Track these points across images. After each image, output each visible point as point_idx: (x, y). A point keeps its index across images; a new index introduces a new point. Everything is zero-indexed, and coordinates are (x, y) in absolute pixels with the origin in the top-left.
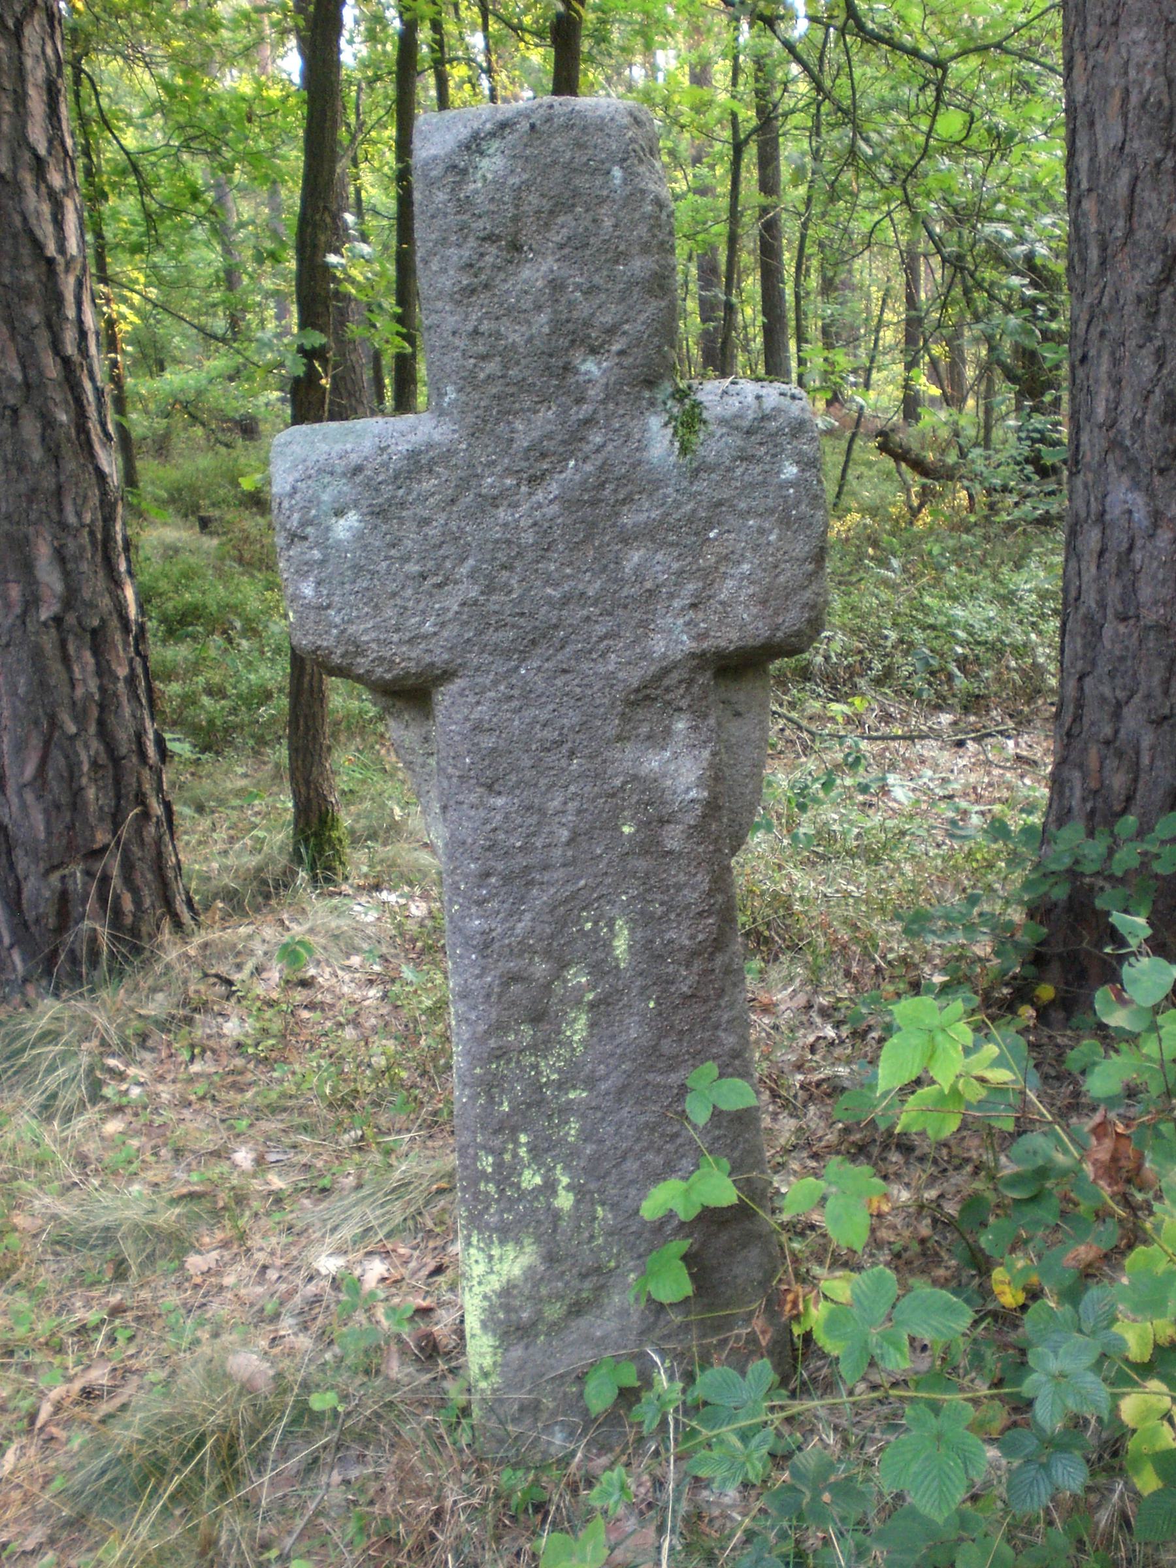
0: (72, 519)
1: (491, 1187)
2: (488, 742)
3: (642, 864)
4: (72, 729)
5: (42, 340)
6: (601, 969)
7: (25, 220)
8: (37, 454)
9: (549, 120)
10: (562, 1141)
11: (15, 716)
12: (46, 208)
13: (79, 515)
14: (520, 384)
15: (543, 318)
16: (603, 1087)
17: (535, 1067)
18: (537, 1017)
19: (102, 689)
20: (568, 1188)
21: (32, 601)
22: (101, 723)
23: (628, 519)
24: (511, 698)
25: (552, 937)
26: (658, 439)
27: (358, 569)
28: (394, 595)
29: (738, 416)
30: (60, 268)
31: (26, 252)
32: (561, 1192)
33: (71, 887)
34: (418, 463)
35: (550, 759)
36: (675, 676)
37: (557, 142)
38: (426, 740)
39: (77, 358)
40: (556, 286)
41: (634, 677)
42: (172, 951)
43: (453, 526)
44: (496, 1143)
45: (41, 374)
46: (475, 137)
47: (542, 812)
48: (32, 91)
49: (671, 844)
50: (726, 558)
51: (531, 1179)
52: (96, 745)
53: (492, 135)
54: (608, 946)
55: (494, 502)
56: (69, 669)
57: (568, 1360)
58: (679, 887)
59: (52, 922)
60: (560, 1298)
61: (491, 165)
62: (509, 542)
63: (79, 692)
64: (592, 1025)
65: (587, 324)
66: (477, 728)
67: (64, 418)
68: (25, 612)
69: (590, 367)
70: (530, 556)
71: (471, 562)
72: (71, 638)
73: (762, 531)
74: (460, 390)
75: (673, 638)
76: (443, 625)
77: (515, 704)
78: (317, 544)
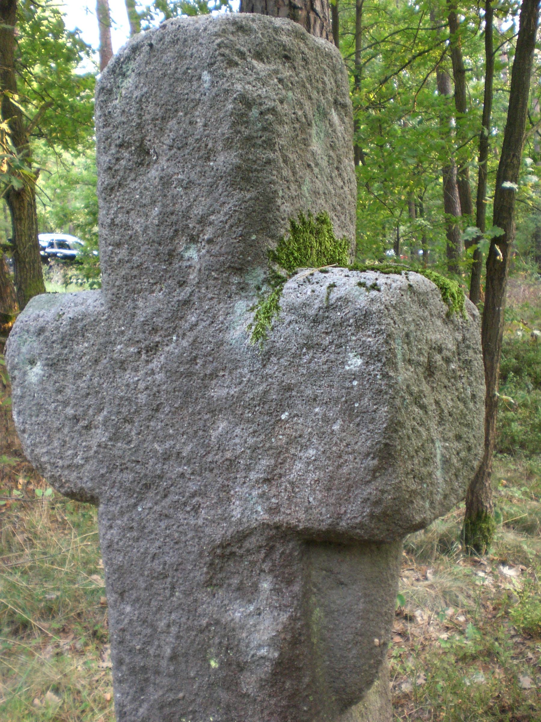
23: (218, 392)
36: (252, 542)
41: (219, 533)
47: (153, 626)
55: (122, 365)
70: (144, 415)
75: (248, 507)
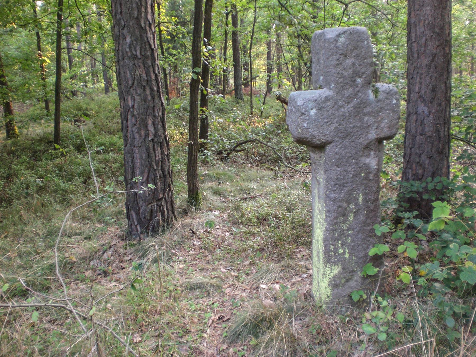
0: (157, 115)
1: (333, 253)
2: (338, 156)
3: (365, 182)
4: (156, 168)
5: (151, 69)
6: (356, 205)
7: (147, 39)
8: (149, 98)
9: (353, 31)
10: (347, 242)
11: (141, 164)
12: (152, 36)
13: (158, 113)
14: (347, 84)
15: (351, 70)
16: (356, 230)
17: (342, 226)
18: (344, 215)
19: (162, 158)
20: (348, 253)
21: (147, 135)
22: (161, 167)
23: (365, 111)
24: (342, 147)
25: (348, 198)
26: (371, 95)
27: (315, 121)
28: (322, 126)
29: (386, 90)
30: (155, 51)
31: (148, 47)
32: (347, 254)
33: (153, 209)
34: (327, 99)
35: (349, 160)
36: (373, 143)
37: (355, 36)
38: (321, 157)
39: (158, 74)
40: (354, 64)
41: (365, 143)
42: (178, 224)
43: (333, 112)
44: (334, 243)
45: (151, 78)
46: (339, 34)
47: (347, 171)
48: (149, 6)
49: (371, 178)
50: (382, 119)
51: (341, 251)
52: (160, 172)
53: (343, 34)
54: (358, 200)
55: (341, 107)
56: (155, 152)
57: (348, 291)
58: (372, 187)
59: (149, 218)
60: (345, 278)
61: (342, 40)
62: (343, 115)
63: (157, 158)
64: (354, 217)
65: (359, 72)
66: (336, 154)
67: (156, 89)
68: (145, 138)
69: (359, 80)
70: (347, 118)
71: (336, 119)
72: (156, 144)
73: (389, 113)
74: (335, 85)
75: (372, 135)
76: (331, 132)
77: (343, 149)
78: (308, 116)
